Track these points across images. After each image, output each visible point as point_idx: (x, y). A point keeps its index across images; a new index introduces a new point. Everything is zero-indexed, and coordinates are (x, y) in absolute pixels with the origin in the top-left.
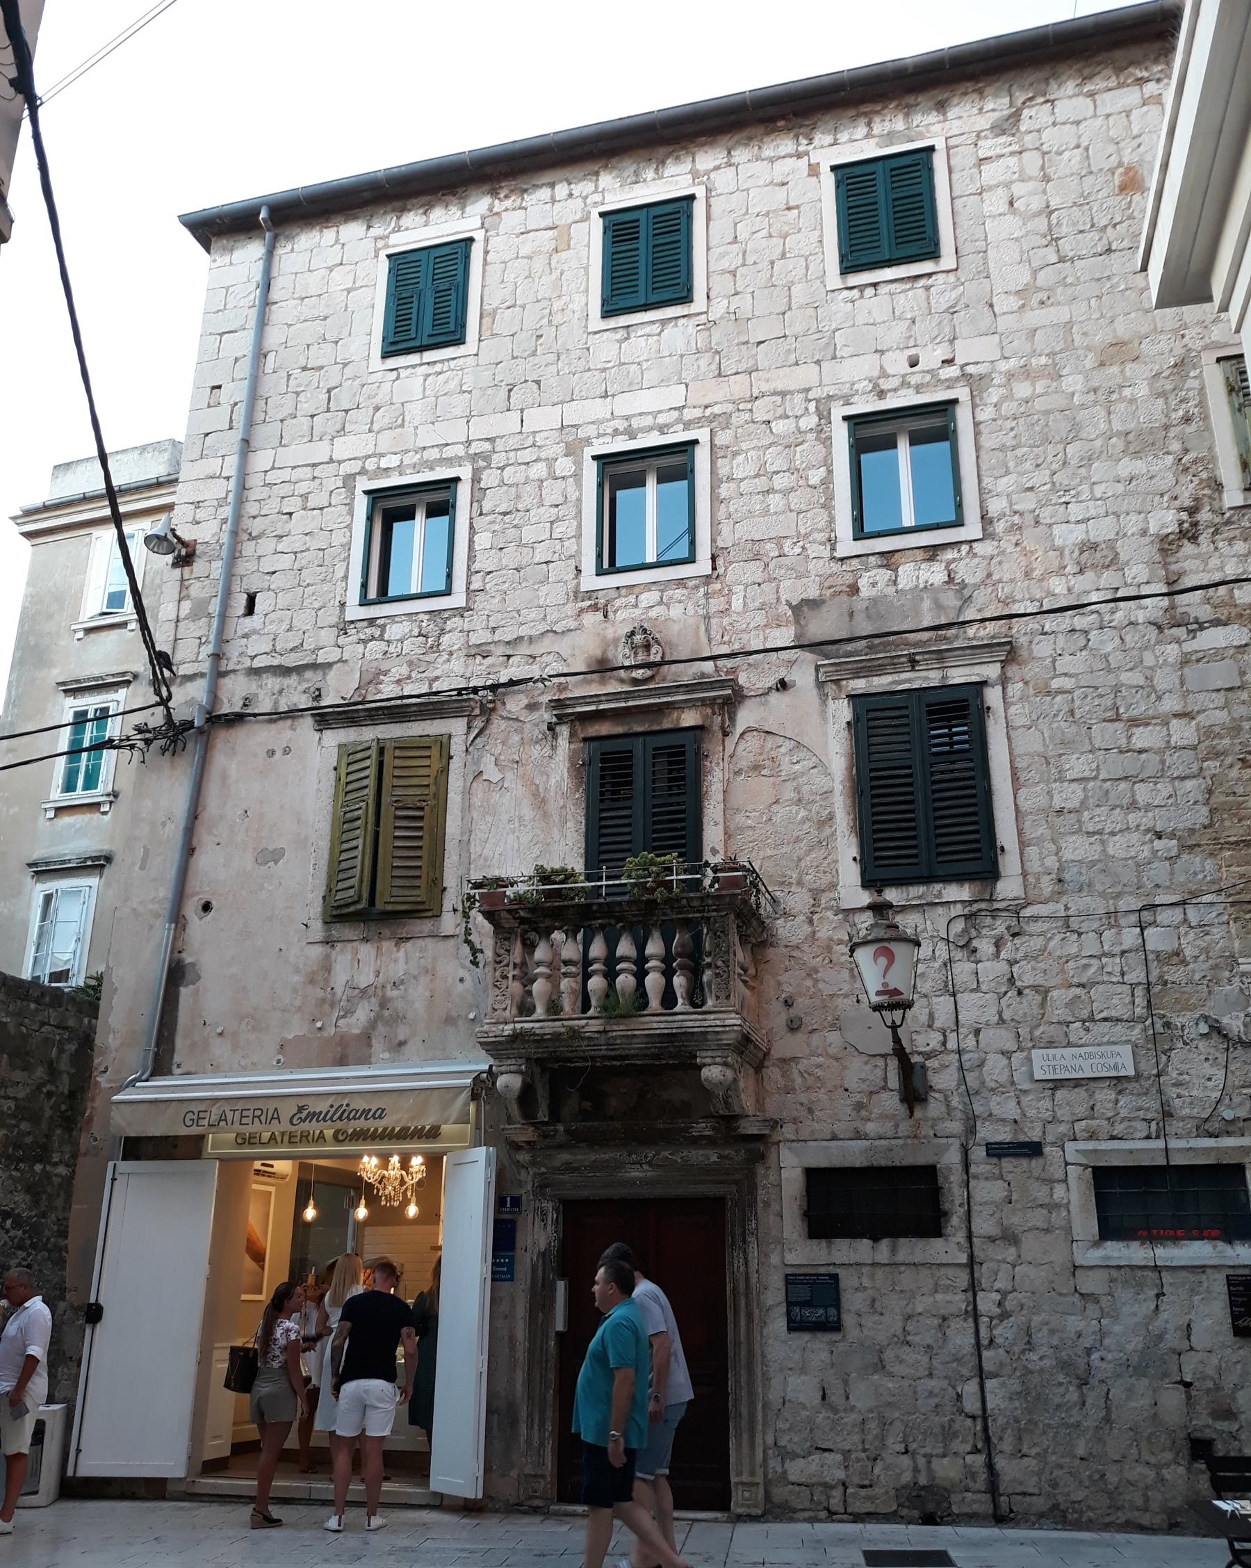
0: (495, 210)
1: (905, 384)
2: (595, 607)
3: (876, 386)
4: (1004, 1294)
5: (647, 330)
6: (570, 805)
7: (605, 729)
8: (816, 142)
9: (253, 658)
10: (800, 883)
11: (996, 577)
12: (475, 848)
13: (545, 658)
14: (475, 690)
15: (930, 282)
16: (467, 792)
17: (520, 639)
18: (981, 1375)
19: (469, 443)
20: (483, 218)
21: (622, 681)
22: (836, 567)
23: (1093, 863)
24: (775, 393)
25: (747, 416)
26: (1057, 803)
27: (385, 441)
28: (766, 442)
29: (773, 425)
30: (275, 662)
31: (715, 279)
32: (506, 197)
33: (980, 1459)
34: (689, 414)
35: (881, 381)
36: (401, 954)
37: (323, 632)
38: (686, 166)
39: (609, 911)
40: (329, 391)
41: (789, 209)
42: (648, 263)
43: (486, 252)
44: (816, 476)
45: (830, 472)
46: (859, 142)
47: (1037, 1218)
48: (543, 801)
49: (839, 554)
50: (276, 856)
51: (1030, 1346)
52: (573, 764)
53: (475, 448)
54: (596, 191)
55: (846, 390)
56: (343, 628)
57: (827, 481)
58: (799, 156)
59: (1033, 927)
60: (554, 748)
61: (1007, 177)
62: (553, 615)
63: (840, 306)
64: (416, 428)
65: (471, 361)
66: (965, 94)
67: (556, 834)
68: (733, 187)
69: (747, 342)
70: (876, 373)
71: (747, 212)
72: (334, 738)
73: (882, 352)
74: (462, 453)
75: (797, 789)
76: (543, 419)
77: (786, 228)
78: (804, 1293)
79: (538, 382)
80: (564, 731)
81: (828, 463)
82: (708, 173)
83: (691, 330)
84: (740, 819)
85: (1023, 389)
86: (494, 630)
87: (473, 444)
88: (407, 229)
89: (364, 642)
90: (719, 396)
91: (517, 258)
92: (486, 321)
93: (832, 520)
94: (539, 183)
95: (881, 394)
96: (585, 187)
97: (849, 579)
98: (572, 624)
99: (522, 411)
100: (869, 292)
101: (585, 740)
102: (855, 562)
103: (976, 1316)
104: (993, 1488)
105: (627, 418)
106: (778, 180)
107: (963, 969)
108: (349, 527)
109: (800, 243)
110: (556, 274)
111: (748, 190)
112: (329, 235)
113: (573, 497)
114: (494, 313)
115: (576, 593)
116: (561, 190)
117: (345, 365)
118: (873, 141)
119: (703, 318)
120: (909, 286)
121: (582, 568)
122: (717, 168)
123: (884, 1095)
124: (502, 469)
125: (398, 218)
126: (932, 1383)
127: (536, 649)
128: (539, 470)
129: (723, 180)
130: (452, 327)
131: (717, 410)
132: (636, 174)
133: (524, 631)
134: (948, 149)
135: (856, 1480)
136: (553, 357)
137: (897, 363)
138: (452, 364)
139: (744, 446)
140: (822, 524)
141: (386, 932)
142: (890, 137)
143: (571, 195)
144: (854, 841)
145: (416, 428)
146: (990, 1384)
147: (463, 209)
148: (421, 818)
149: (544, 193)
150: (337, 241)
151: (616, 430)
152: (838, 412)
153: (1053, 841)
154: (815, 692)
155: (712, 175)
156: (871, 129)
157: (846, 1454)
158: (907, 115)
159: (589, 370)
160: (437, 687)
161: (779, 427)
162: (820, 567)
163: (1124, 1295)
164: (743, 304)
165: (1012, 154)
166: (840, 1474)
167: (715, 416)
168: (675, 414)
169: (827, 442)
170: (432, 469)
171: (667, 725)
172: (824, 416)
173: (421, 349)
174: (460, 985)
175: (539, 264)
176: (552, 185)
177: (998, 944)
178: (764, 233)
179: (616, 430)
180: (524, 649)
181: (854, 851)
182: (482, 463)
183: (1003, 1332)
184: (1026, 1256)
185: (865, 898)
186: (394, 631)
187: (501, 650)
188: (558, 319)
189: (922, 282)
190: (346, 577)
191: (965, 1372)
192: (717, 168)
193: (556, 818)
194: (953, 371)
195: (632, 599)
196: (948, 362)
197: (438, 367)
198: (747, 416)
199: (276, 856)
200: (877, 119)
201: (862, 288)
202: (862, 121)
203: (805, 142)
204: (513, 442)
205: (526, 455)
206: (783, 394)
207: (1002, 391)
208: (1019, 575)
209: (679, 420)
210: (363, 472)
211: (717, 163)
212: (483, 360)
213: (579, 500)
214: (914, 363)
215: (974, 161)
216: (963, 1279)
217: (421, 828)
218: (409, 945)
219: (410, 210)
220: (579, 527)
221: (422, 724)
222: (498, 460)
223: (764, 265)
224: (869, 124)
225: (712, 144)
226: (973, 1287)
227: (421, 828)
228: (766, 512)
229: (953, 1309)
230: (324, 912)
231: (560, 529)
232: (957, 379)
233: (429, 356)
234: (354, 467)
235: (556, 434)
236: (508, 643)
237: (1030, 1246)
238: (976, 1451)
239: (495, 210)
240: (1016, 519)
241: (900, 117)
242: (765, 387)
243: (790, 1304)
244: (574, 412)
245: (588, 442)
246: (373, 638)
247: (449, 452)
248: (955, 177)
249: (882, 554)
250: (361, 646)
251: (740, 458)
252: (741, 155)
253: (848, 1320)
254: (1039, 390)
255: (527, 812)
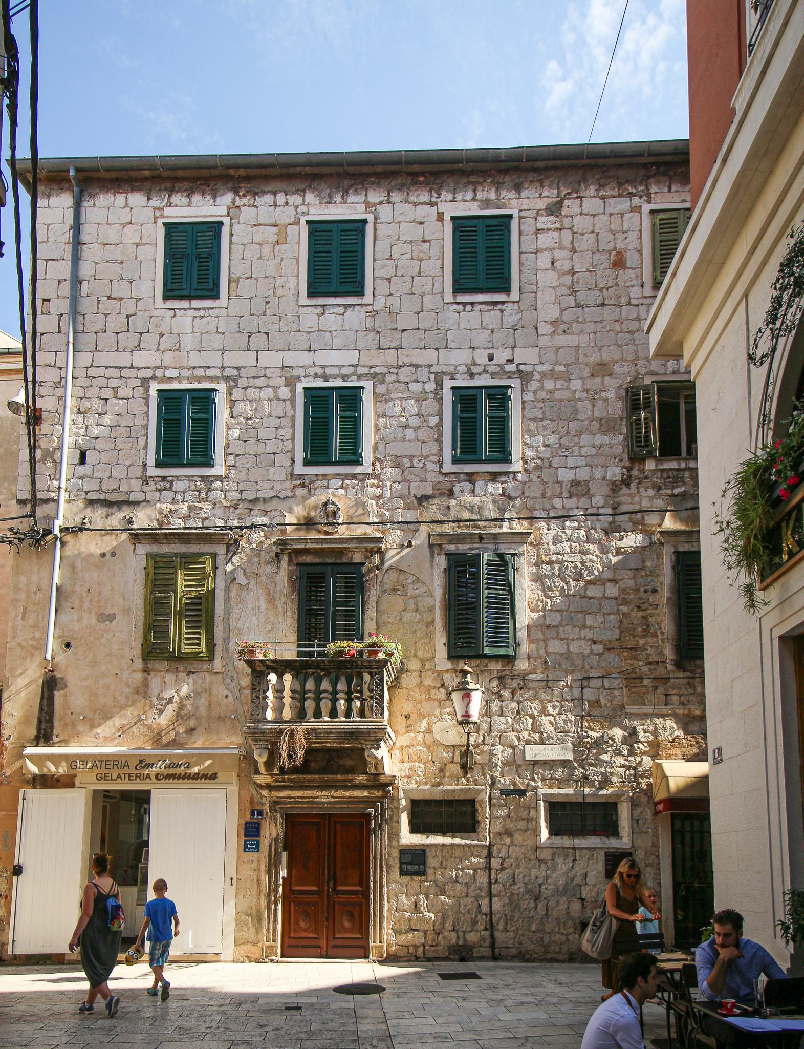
0: (237, 204)
1: (485, 371)
2: (303, 485)
3: (469, 369)
4: (504, 860)
5: (337, 310)
6: (289, 602)
7: (309, 559)
8: (443, 197)
9: (87, 493)
10: (415, 656)
11: (526, 494)
12: (233, 623)
13: (273, 513)
14: (231, 529)
15: (504, 307)
16: (227, 590)
17: (258, 499)
18: (491, 896)
19: (223, 368)
20: (229, 208)
21: (319, 532)
22: (441, 478)
23: (561, 655)
24: (411, 365)
25: (394, 377)
26: (548, 622)
27: (168, 359)
28: (405, 396)
29: (410, 385)
30: (102, 497)
31: (378, 282)
32: (244, 196)
33: (487, 933)
34: (361, 370)
35: (472, 367)
36: (191, 681)
37: (132, 481)
38: (361, 198)
39: (317, 666)
40: (128, 317)
41: (424, 241)
42: (336, 264)
43: (232, 235)
44: (433, 421)
45: (441, 420)
46: (466, 204)
47: (522, 825)
48: (273, 599)
49: (444, 470)
50: (111, 618)
51: (514, 883)
52: (290, 578)
53: (228, 372)
54: (303, 204)
55: (452, 369)
56: (146, 480)
57: (440, 425)
58: (432, 204)
59: (531, 685)
60: (278, 568)
61: (553, 245)
62: (278, 486)
63: (451, 316)
64: (188, 353)
65: (224, 312)
66: (532, 182)
67: (281, 619)
68: (390, 219)
69: (396, 329)
70: (470, 361)
71: (398, 239)
72: (143, 550)
73: (474, 349)
74: (219, 375)
75: (416, 604)
76: (270, 359)
77: (422, 255)
78: (408, 858)
79: (267, 334)
80: (285, 559)
81: (440, 414)
82: (375, 205)
83: (363, 315)
84: (385, 618)
85: (549, 384)
86: (241, 492)
87: (227, 370)
88: (176, 206)
89: (160, 491)
90: (378, 362)
91: (252, 243)
92: (233, 285)
93: (441, 450)
94: (266, 190)
95: (472, 376)
96: (295, 199)
97: (449, 486)
98: (290, 494)
99: (257, 351)
100: (469, 308)
101: (297, 564)
102: (452, 476)
103: (490, 869)
104: (493, 945)
105: (323, 367)
106: (418, 219)
107: (495, 706)
108: (147, 414)
109: (431, 266)
110: (278, 260)
111: (399, 223)
112: (120, 199)
113: (290, 413)
114: (237, 281)
115: (292, 474)
116: (281, 198)
117: (138, 300)
118: (477, 204)
119: (370, 308)
120: (491, 308)
121: (296, 459)
122: (381, 203)
123: (452, 765)
124: (245, 388)
125: (170, 196)
126: (466, 900)
127: (268, 507)
128: (269, 392)
129: (385, 212)
130: (211, 286)
131: (377, 370)
132: (330, 196)
133: (260, 495)
134: (520, 218)
135: (430, 943)
136: (277, 318)
137: (481, 357)
138: (211, 312)
139: (392, 396)
140: (435, 451)
141: (181, 668)
142: (486, 204)
143: (287, 203)
144: (445, 634)
145: (188, 353)
146: (495, 900)
147: (215, 198)
148: (200, 604)
149: (269, 198)
150: (127, 205)
151: (316, 374)
152: (448, 384)
153: (544, 641)
154: (428, 549)
155: (378, 207)
156: (476, 195)
157: (425, 932)
158: (497, 190)
159: (299, 331)
160: (206, 524)
161: (414, 387)
162: (433, 477)
163: (559, 861)
164: (395, 301)
165: (556, 229)
166: (423, 940)
167: (376, 374)
168: (352, 369)
169: (440, 401)
170: (199, 382)
171: (345, 560)
172: (440, 384)
173: (190, 297)
174: (225, 700)
175: (267, 250)
176: (275, 193)
177: (513, 693)
178: (408, 256)
179: (316, 374)
180: (260, 506)
181: (444, 640)
182: (232, 384)
183: (502, 877)
184: (516, 842)
185: (449, 665)
186: (179, 486)
187: (246, 505)
188: (279, 292)
189: (499, 307)
190: (146, 447)
191: (483, 894)
192: (381, 203)
193: (280, 609)
194: (511, 368)
195: (325, 483)
196: (510, 361)
197: (202, 313)
198: (394, 377)
199: (111, 618)
200: (480, 188)
201: (465, 304)
202: (471, 188)
203: (435, 195)
204: (253, 372)
205: (260, 382)
206: (416, 366)
207: (538, 384)
208: (539, 495)
209: (354, 374)
210: (154, 377)
211: (381, 199)
212: (232, 312)
213: (294, 416)
214: (491, 358)
215: (533, 230)
216: (485, 852)
217: (200, 610)
218: (194, 675)
219: (177, 192)
220: (294, 433)
221: (199, 546)
222: (242, 382)
223: (408, 278)
224: (474, 191)
225: (378, 184)
226: (490, 856)
227: (200, 610)
228: (404, 440)
229: (480, 866)
230: (142, 654)
231: (281, 432)
232: (514, 373)
233: (196, 304)
234: (148, 374)
235: (279, 371)
236: (250, 501)
237: (518, 837)
238: (486, 929)
239: (237, 204)
240: (539, 462)
241: (494, 189)
242: (407, 360)
243: (401, 863)
244: (291, 358)
245: (298, 379)
246: (165, 489)
247: (210, 373)
248: (523, 238)
249: (467, 474)
250: (158, 493)
251: (391, 404)
252: (396, 197)
253: (430, 871)
254: (558, 386)
255: (263, 605)
